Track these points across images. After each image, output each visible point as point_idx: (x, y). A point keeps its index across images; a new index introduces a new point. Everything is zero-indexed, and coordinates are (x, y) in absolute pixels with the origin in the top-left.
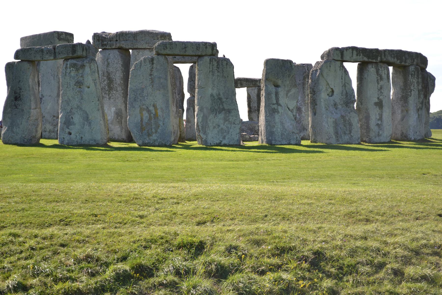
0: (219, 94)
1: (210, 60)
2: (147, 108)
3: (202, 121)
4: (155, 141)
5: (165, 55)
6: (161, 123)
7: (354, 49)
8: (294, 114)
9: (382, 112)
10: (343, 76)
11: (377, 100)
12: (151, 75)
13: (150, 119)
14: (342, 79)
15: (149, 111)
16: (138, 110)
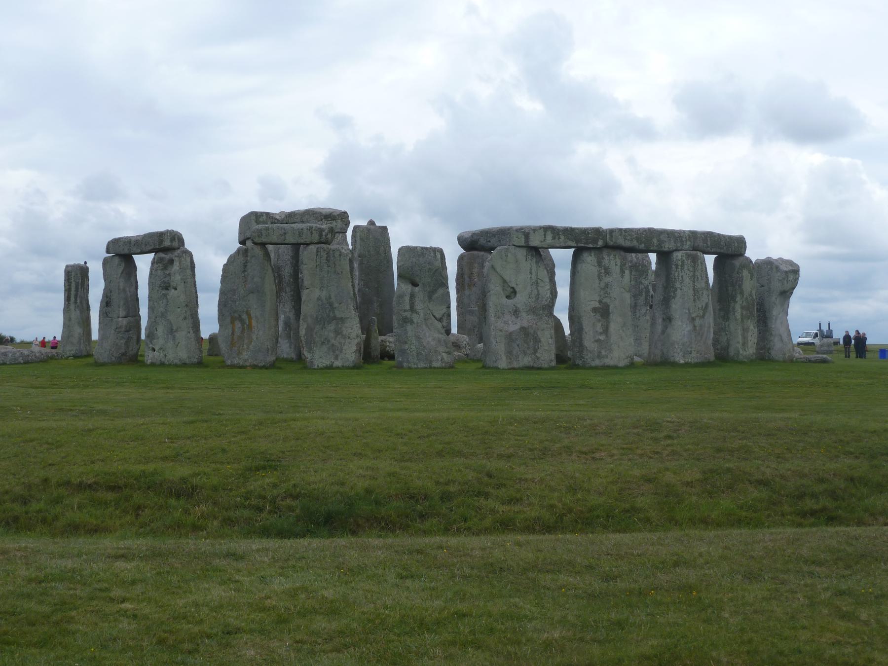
0: (330, 298)
1: (317, 251)
2: (240, 316)
3: (306, 334)
4: (246, 361)
5: (263, 245)
6: (254, 337)
7: (547, 229)
8: (445, 324)
9: (608, 322)
10: (534, 269)
11: (597, 305)
12: (244, 271)
13: (243, 331)
14: (531, 273)
15: (242, 321)
16: (228, 320)
